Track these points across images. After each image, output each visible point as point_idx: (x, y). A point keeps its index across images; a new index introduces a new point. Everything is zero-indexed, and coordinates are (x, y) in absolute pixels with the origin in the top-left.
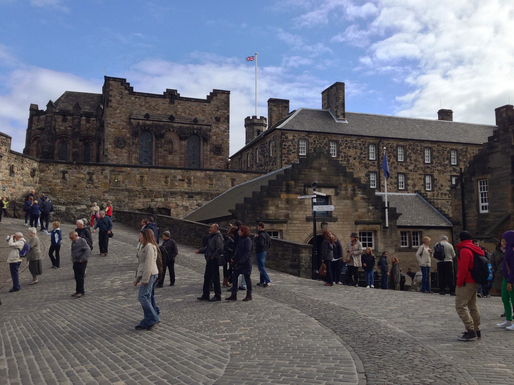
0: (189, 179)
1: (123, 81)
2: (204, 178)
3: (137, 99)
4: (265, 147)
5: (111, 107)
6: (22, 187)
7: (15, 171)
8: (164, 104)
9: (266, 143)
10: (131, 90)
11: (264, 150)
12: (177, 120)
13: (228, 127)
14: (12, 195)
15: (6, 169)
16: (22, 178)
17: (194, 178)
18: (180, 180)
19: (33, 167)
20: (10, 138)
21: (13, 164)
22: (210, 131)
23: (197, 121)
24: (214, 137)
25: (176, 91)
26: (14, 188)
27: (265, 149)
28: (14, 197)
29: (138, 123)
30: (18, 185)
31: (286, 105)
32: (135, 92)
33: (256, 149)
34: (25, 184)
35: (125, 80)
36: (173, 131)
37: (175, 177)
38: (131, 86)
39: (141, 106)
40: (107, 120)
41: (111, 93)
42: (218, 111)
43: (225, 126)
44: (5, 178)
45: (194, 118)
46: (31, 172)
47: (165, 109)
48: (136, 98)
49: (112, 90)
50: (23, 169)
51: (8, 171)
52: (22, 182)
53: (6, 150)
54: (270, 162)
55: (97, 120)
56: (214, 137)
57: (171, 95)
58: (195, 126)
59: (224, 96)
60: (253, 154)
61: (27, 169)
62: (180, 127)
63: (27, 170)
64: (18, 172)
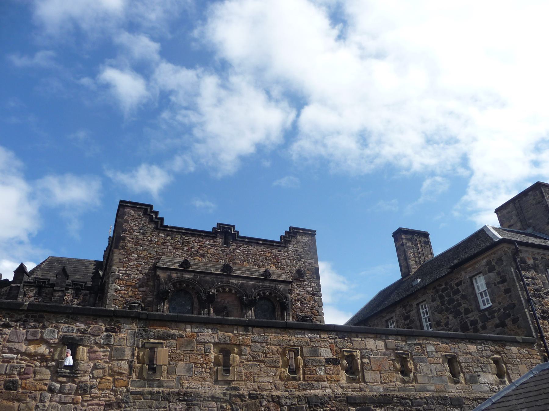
0: (351, 358)
1: (146, 210)
2: (385, 355)
3: (169, 238)
4: (457, 292)
5: (123, 248)
8: (215, 247)
9: (458, 285)
10: (158, 223)
11: (451, 301)
12: (236, 273)
13: (319, 286)
17: (362, 357)
18: (328, 361)
22: (291, 292)
23: (270, 275)
24: (298, 303)
25: (234, 226)
27: (458, 297)
29: (170, 278)
31: (425, 239)
32: (167, 226)
33: (418, 305)
35: (151, 206)
36: (230, 290)
37: (315, 352)
38: (160, 216)
39: (175, 248)
40: (115, 270)
41: (126, 226)
42: (300, 260)
43: (313, 285)
45: (263, 270)
47: (215, 255)
48: (167, 235)
49: (127, 222)
54: (485, 319)
55: (90, 294)
56: (298, 303)
57: (225, 233)
58: (267, 284)
59: (306, 239)
60: (407, 318)
62: (242, 285)
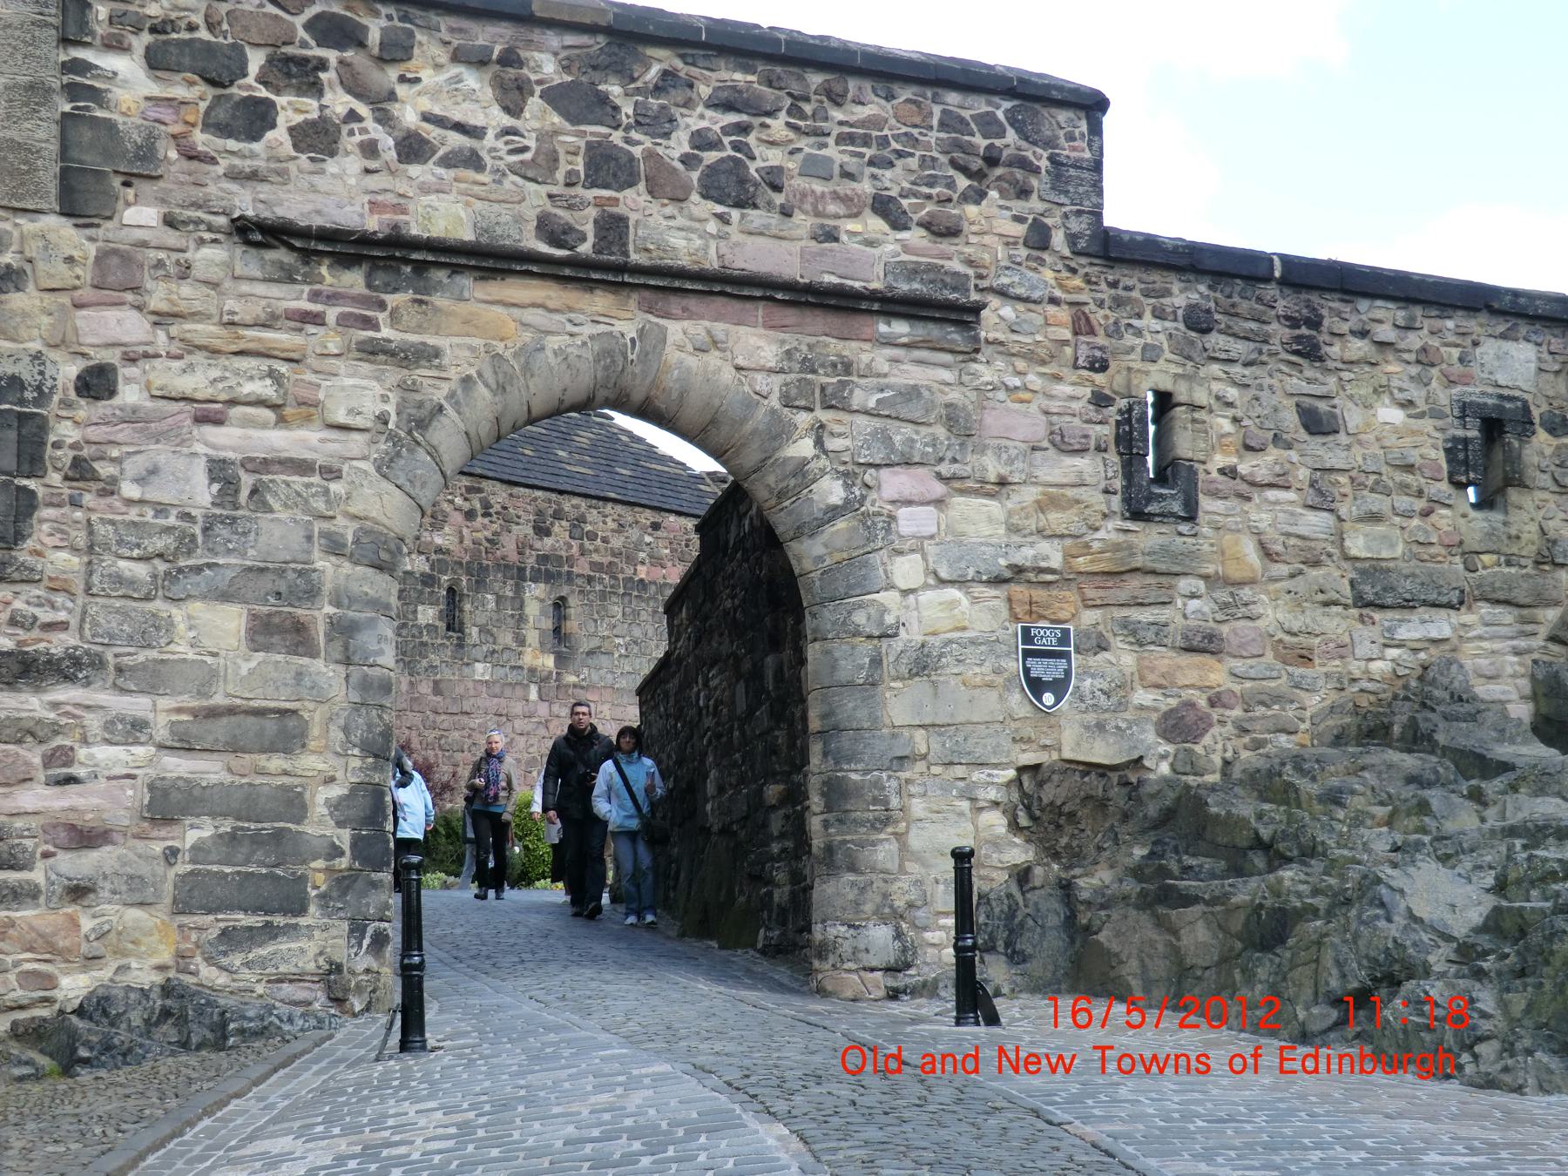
6: (1336, 624)
7: (1209, 444)
14: (1180, 726)
15: (1062, 444)
16: (1316, 523)
19: (1473, 393)
20: (1092, 105)
21: (1161, 375)
26: (1203, 645)
28: (1215, 745)
30: (1273, 613)
34: (1375, 593)
44: (1053, 555)
46: (1456, 450)
50: (1317, 423)
51: (1094, 472)
52: (1337, 578)
53: (1039, 238)
61: (1391, 415)
63: (1392, 417)
64: (1257, 466)
